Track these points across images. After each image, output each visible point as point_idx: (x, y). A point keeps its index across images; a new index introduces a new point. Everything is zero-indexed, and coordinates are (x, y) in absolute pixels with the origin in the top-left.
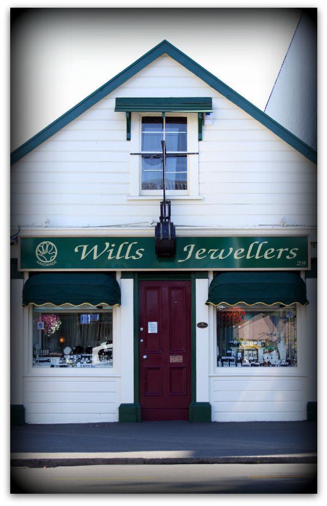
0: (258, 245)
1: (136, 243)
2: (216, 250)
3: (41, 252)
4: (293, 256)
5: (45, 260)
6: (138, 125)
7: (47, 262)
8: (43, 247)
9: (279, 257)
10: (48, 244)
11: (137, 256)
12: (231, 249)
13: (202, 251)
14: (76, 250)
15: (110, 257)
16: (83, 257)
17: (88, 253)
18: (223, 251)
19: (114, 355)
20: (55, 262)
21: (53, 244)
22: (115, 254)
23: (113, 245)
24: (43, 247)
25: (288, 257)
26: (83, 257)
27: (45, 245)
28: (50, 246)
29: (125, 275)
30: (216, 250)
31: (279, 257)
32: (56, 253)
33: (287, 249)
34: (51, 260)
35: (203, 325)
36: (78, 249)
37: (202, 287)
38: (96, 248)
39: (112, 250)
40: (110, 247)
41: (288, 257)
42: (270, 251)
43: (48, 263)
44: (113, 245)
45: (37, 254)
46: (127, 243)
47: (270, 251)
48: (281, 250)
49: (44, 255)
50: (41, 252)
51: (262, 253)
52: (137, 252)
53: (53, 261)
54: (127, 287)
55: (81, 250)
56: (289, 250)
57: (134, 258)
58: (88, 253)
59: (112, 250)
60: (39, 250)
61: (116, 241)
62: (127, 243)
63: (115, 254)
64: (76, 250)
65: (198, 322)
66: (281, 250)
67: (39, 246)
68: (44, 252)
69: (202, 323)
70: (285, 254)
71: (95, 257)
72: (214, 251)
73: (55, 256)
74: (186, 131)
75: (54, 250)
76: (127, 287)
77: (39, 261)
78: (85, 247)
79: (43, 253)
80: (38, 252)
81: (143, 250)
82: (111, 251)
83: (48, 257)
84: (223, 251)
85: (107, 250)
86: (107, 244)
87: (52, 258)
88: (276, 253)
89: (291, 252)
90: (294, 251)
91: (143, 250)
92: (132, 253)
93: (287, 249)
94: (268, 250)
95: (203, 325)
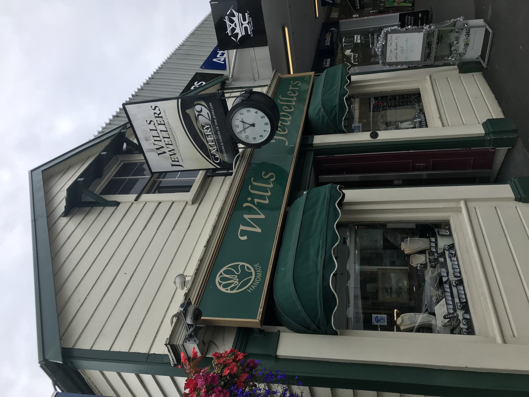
3: (232, 286)
8: (224, 283)
14: (245, 238)
24: (224, 283)
26: (259, 230)
28: (226, 272)
34: (253, 271)
36: (241, 236)
40: (252, 202)
43: (256, 275)
45: (234, 291)
49: (239, 282)
50: (232, 286)
53: (254, 268)
55: (243, 233)
60: (229, 288)
64: (245, 238)
67: (221, 288)
68: (235, 281)
75: (235, 267)
77: (248, 288)
78: (242, 227)
80: (232, 289)
82: (256, 200)
83: (244, 275)
87: (248, 268)
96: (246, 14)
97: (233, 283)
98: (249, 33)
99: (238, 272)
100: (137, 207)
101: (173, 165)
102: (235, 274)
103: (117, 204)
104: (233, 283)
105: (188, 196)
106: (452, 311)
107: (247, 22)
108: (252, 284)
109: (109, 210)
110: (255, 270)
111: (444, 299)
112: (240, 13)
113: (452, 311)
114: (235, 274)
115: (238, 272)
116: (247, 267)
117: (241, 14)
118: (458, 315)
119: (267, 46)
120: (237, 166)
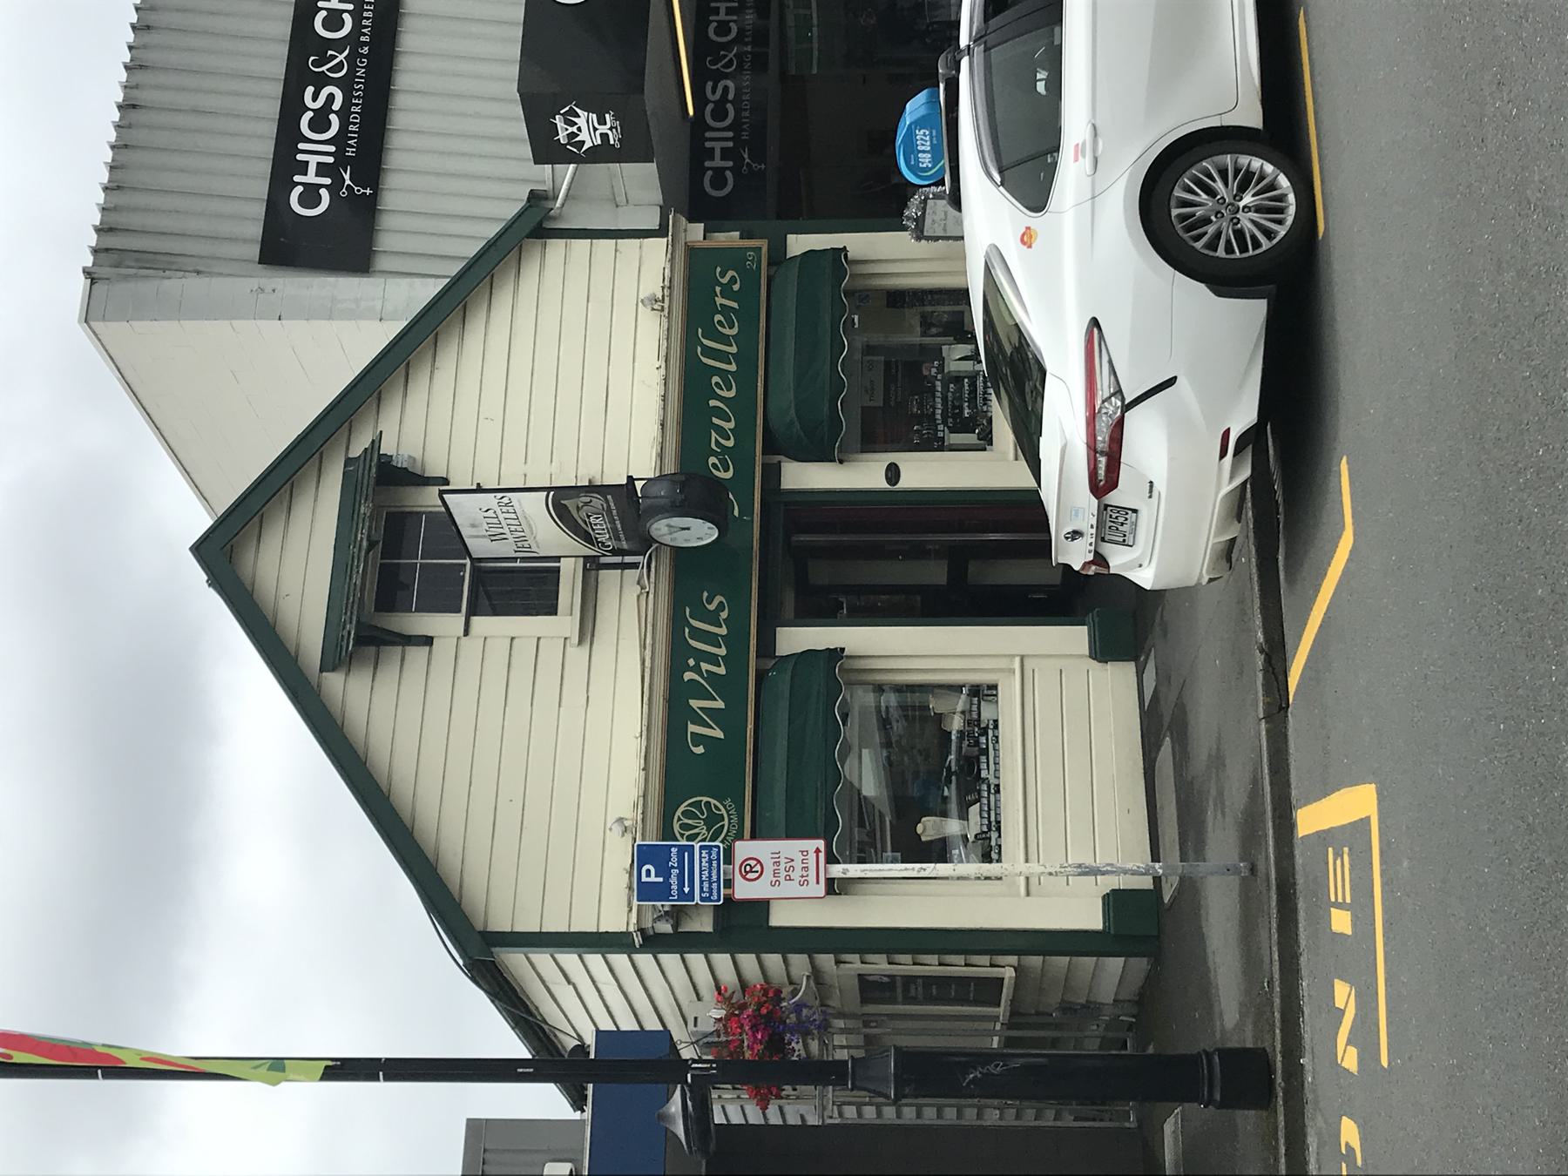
0: (692, 628)
1: (688, 610)
2: (713, 434)
4: (721, 602)
5: (723, 826)
6: (392, 619)
7: (726, 822)
8: (687, 833)
9: (735, 305)
10: (679, 819)
11: (721, 607)
12: (713, 403)
13: (717, 384)
14: (700, 750)
15: (722, 671)
16: (719, 734)
17: (711, 723)
18: (715, 420)
19: (965, 238)
20: (728, 802)
21: (682, 808)
22: (713, 659)
23: (691, 662)
24: (687, 833)
25: (736, 287)
26: (719, 734)
27: (685, 827)
29: (767, 644)
30: (713, 434)
31: (735, 305)
32: (705, 799)
33: (718, 289)
34: (724, 811)
35: (893, 473)
37: (805, 476)
38: (694, 703)
39: (702, 664)
41: (736, 287)
42: (714, 465)
43: (730, 819)
44: (691, 662)
46: (687, 630)
47: (714, 465)
48: (719, 301)
49: (708, 830)
51: (725, 340)
52: (711, 607)
53: (725, 807)
54: (796, 639)
56: (721, 284)
57: (724, 615)
58: (711, 723)
59: (702, 664)
61: (678, 654)
62: (687, 630)
63: (713, 659)
64: (700, 750)
65: (883, 485)
66: (719, 301)
69: (886, 475)
70: (727, 292)
71: (720, 704)
72: (716, 440)
73: (713, 801)
74: (419, 514)
75: (697, 805)
76: (796, 639)
78: (692, 728)
79: (704, 831)
81: (705, 594)
82: (704, 666)
84: (715, 420)
85: (702, 677)
86: (688, 676)
87: (716, 806)
88: (725, 310)
89: (725, 281)
90: (723, 275)
91: (705, 594)
92: (713, 619)
93: (718, 289)
94: (719, 328)
95: (893, 473)
96: (607, 116)
97: (699, 834)
98: (612, 142)
99: (703, 814)
100: (471, 646)
101: (516, 551)
102: (700, 819)
103: (428, 641)
104: (699, 834)
105: (564, 623)
106: (985, 829)
107: (608, 126)
108: (727, 835)
109: (417, 654)
110: (728, 812)
111: (978, 804)
112: (593, 113)
113: (985, 829)
114: (700, 819)
115: (703, 814)
116: (723, 825)
117: (595, 116)
118: (990, 839)
119: (653, 162)
120: (652, 579)
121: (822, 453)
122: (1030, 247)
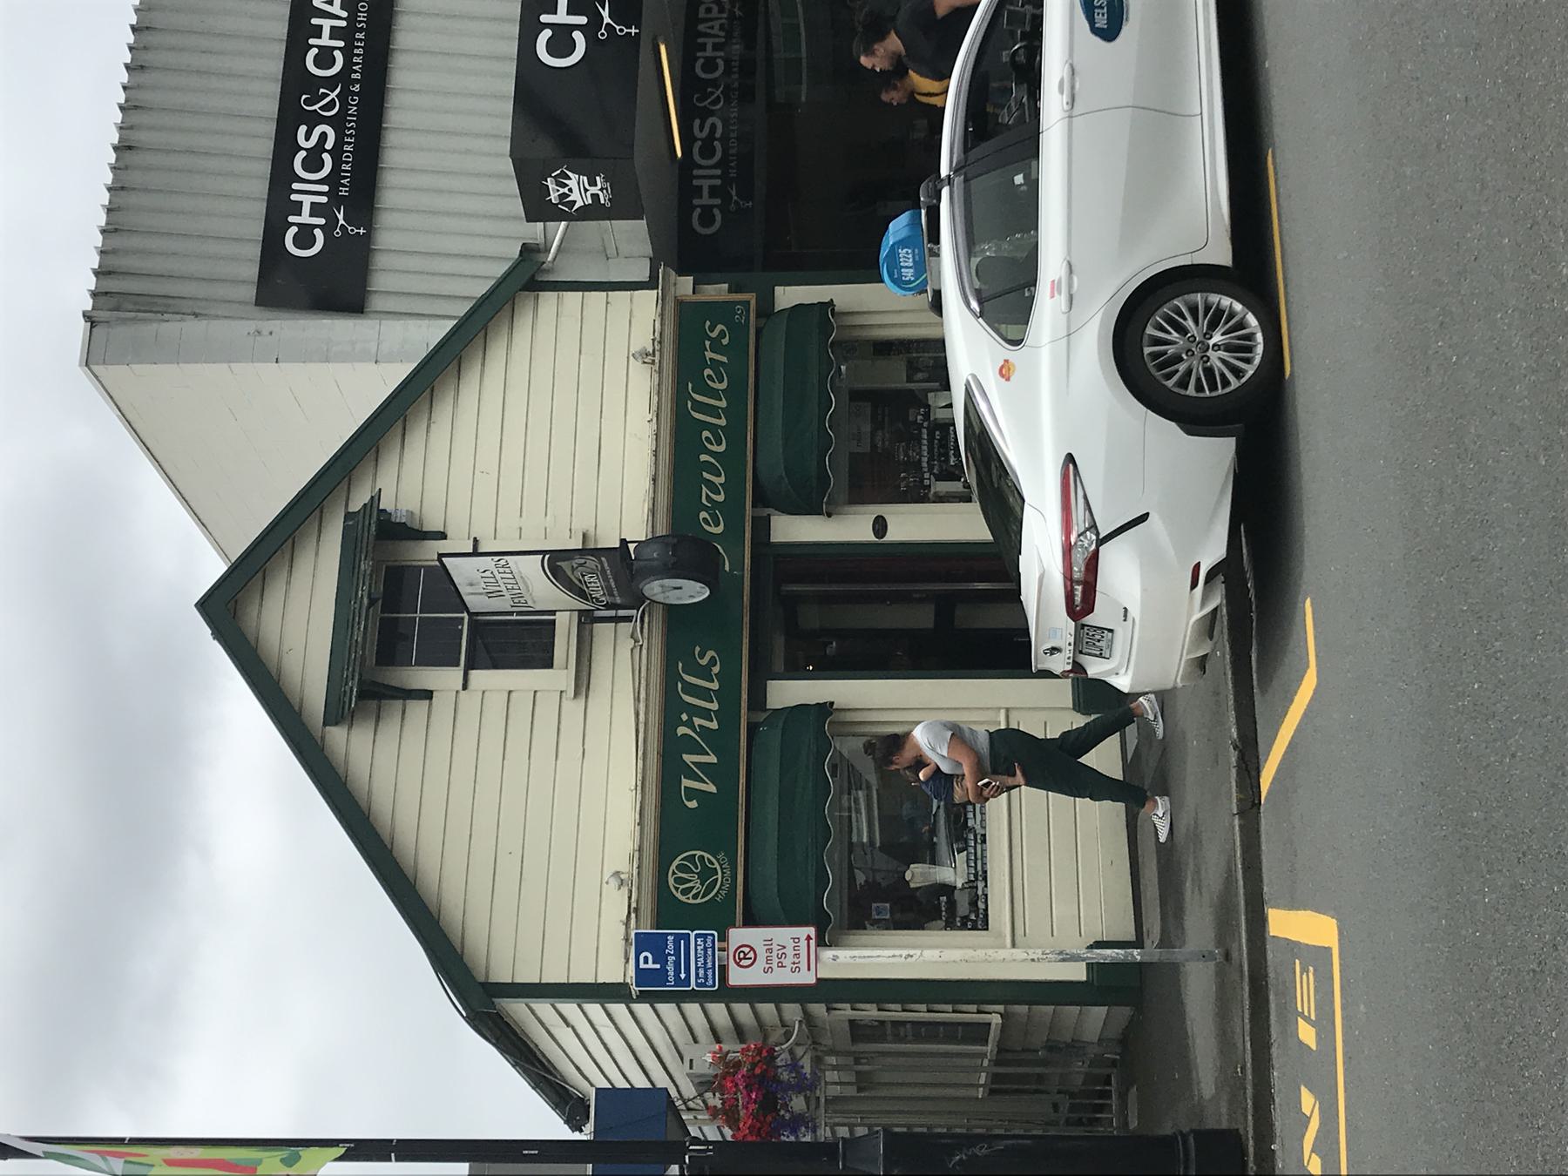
3: (694, 891)
8: (682, 887)
9: (724, 359)
10: (674, 873)
11: (712, 662)
12: (704, 457)
14: (693, 804)
15: (714, 725)
16: (712, 788)
22: (705, 713)
23: (684, 717)
24: (682, 887)
25: (725, 341)
26: (712, 788)
27: (679, 881)
28: (680, 868)
29: (758, 698)
32: (699, 853)
33: (707, 343)
34: (717, 865)
35: (880, 526)
36: (688, 800)
37: (794, 529)
38: (688, 758)
40: (690, 724)
41: (725, 341)
43: (723, 873)
44: (684, 717)
45: (698, 901)
46: (680, 685)
48: (709, 355)
50: (694, 891)
51: (714, 394)
52: (704, 662)
53: (718, 860)
54: (787, 693)
55: (692, 794)
56: (710, 338)
57: (716, 669)
60: (690, 895)
61: (671, 709)
62: (680, 685)
63: (705, 713)
64: (693, 804)
65: (872, 538)
66: (709, 355)
67: (679, 895)
68: (696, 884)
69: (874, 529)
71: (713, 759)
72: (707, 495)
73: (706, 855)
74: (419, 568)
76: (787, 693)
77: (716, 895)
78: (686, 783)
79: (698, 885)
80: (695, 897)
81: (698, 649)
82: (697, 721)
83: (706, 873)
85: (695, 731)
86: (682, 730)
88: (715, 365)
89: (714, 335)
91: (698, 649)
93: (707, 343)
94: (708, 382)
95: (880, 526)
96: (598, 178)
97: (693, 887)
98: (602, 202)
99: (697, 868)
100: (469, 701)
101: (512, 606)
102: (694, 872)
103: (427, 695)
104: (693, 887)
105: (560, 677)
106: (973, 879)
107: (599, 187)
108: (720, 889)
109: (417, 708)
110: (721, 865)
111: (965, 852)
112: (584, 175)
113: (973, 879)
114: (694, 872)
115: (697, 868)
116: (717, 879)
117: (585, 178)
118: (977, 887)
119: (643, 219)
120: (646, 635)
121: (811, 505)
122: (1008, 379)
